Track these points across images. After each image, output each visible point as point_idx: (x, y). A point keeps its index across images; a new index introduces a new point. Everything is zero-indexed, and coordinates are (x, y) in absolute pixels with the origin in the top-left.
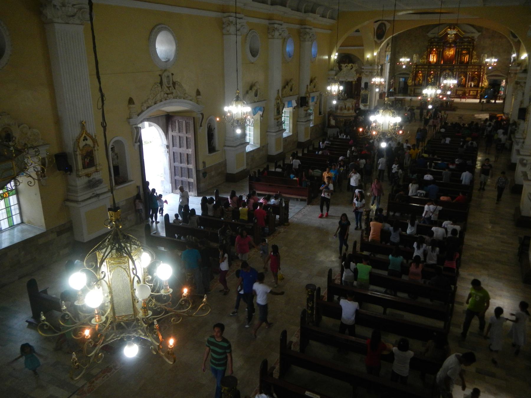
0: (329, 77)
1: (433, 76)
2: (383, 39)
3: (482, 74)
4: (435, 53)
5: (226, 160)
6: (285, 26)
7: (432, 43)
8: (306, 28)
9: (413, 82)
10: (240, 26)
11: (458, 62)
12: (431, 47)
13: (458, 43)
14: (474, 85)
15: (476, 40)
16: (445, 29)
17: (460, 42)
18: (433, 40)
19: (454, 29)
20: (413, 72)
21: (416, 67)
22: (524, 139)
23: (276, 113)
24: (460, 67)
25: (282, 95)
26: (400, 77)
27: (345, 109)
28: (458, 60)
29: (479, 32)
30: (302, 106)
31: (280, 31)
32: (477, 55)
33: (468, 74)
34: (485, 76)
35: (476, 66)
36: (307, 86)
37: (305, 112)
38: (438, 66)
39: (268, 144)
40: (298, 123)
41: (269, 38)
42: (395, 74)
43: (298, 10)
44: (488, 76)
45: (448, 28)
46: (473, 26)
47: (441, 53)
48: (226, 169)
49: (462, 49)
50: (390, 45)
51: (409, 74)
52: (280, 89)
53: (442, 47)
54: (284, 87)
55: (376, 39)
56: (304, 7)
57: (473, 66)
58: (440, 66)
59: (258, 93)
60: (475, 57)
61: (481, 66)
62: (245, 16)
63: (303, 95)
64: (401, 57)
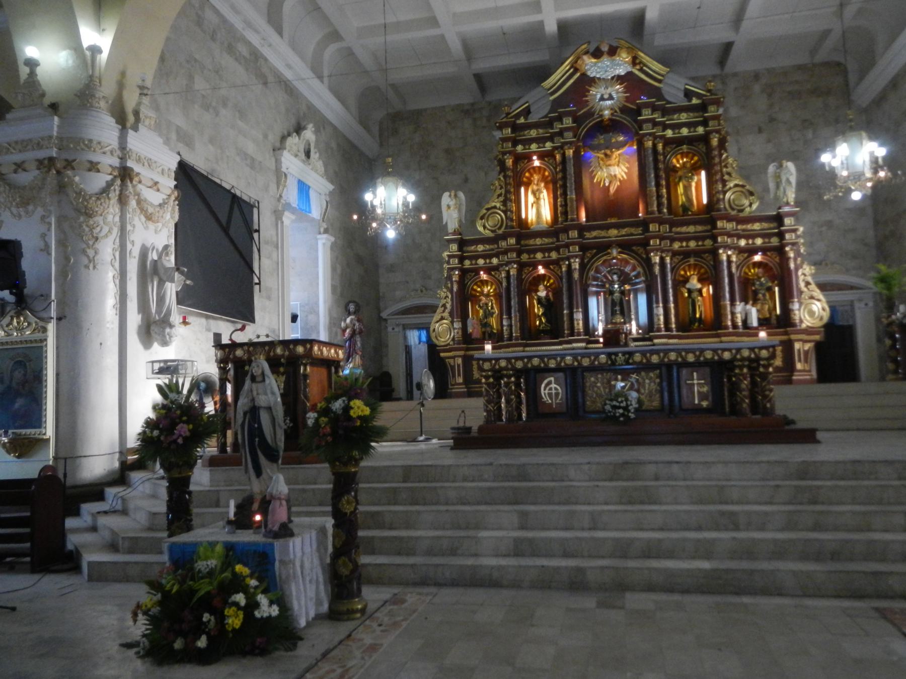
1: (546, 287)
3: (792, 255)
4: (544, 179)
9: (458, 325)
11: (660, 205)
12: (520, 148)
13: (646, 114)
14: (759, 320)
19: (613, 52)
21: (460, 249)
24: (674, 229)
26: (406, 327)
28: (659, 197)
33: (724, 258)
38: (566, 230)
42: (384, 315)
45: (586, 53)
47: (571, 169)
49: (667, 142)
50: (309, 134)
53: (569, 136)
58: (573, 227)
61: (779, 219)
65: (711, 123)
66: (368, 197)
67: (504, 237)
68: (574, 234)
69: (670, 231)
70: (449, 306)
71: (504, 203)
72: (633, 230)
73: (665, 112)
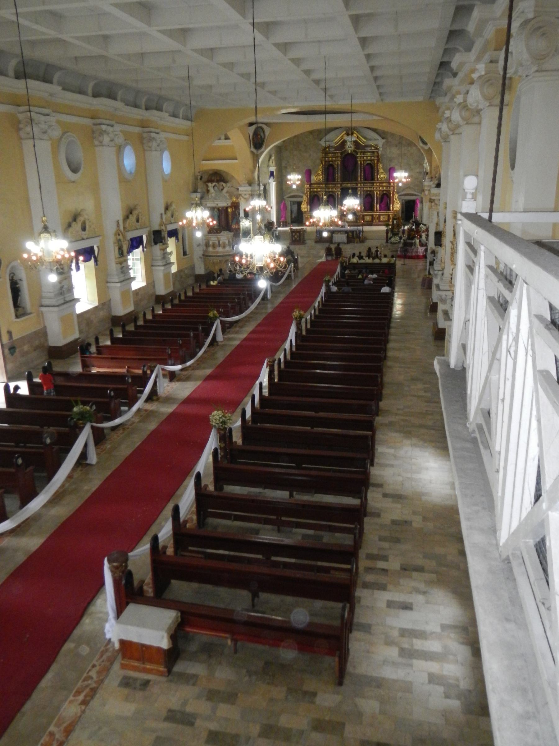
0: (193, 202)
2: (263, 149)
5: (45, 327)
6: (118, 128)
7: (326, 153)
8: (151, 132)
10: (47, 127)
13: (359, 154)
15: (381, 149)
16: (342, 134)
17: (361, 152)
18: (328, 150)
19: (352, 134)
20: (307, 193)
21: (310, 186)
22: (443, 269)
23: (117, 256)
25: (124, 228)
27: (219, 245)
29: (383, 138)
30: (156, 243)
31: (111, 135)
32: (383, 170)
33: (375, 193)
34: (396, 196)
35: (384, 183)
36: (162, 214)
37: (162, 252)
39: (110, 300)
40: (154, 268)
41: (96, 146)
42: (285, 197)
43: (136, 106)
44: (401, 196)
46: (375, 130)
48: (47, 340)
49: (364, 160)
50: (273, 158)
51: (302, 197)
52: (120, 217)
53: (339, 158)
54: (126, 218)
55: (253, 149)
56: (144, 100)
57: (380, 183)
58: (339, 184)
59: (87, 227)
60: (381, 170)
62: (53, 112)
63: (157, 228)
64: (289, 173)
65: (375, 157)
66: (289, 177)
67: (322, 184)
68: (340, 185)
69: (363, 185)
70: (306, 201)
71: (322, 173)
72: (354, 185)
73: (364, 153)
